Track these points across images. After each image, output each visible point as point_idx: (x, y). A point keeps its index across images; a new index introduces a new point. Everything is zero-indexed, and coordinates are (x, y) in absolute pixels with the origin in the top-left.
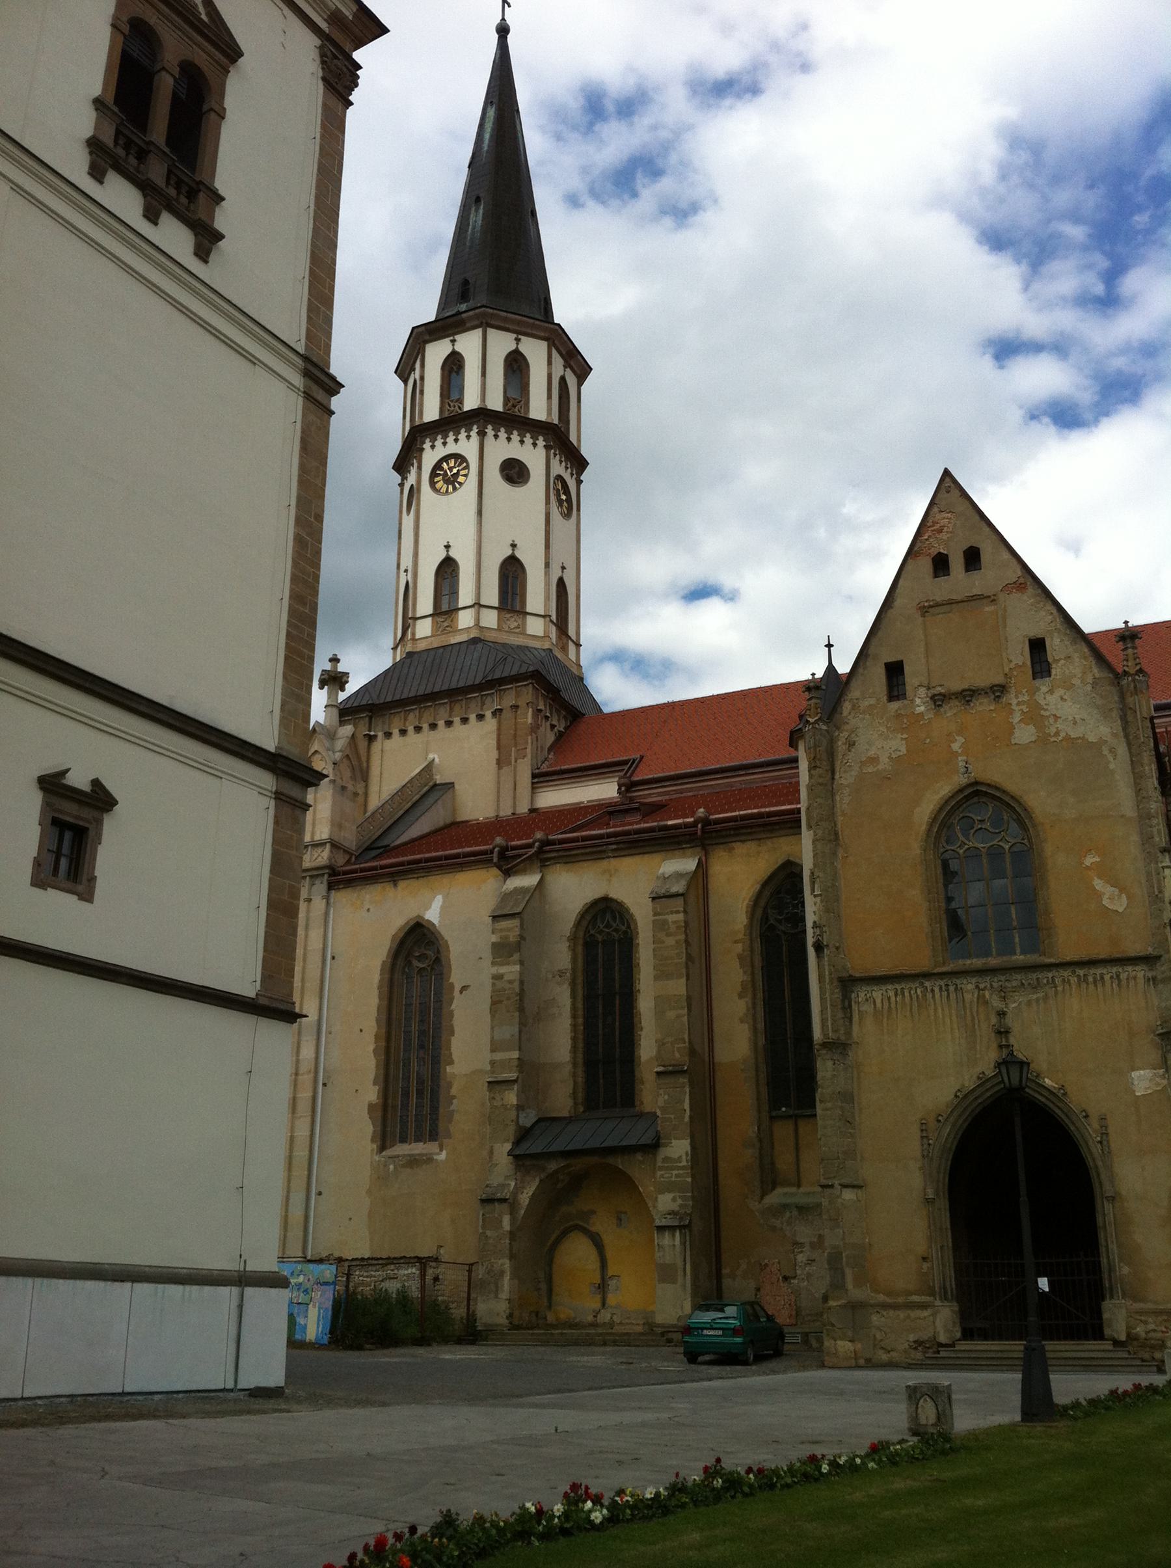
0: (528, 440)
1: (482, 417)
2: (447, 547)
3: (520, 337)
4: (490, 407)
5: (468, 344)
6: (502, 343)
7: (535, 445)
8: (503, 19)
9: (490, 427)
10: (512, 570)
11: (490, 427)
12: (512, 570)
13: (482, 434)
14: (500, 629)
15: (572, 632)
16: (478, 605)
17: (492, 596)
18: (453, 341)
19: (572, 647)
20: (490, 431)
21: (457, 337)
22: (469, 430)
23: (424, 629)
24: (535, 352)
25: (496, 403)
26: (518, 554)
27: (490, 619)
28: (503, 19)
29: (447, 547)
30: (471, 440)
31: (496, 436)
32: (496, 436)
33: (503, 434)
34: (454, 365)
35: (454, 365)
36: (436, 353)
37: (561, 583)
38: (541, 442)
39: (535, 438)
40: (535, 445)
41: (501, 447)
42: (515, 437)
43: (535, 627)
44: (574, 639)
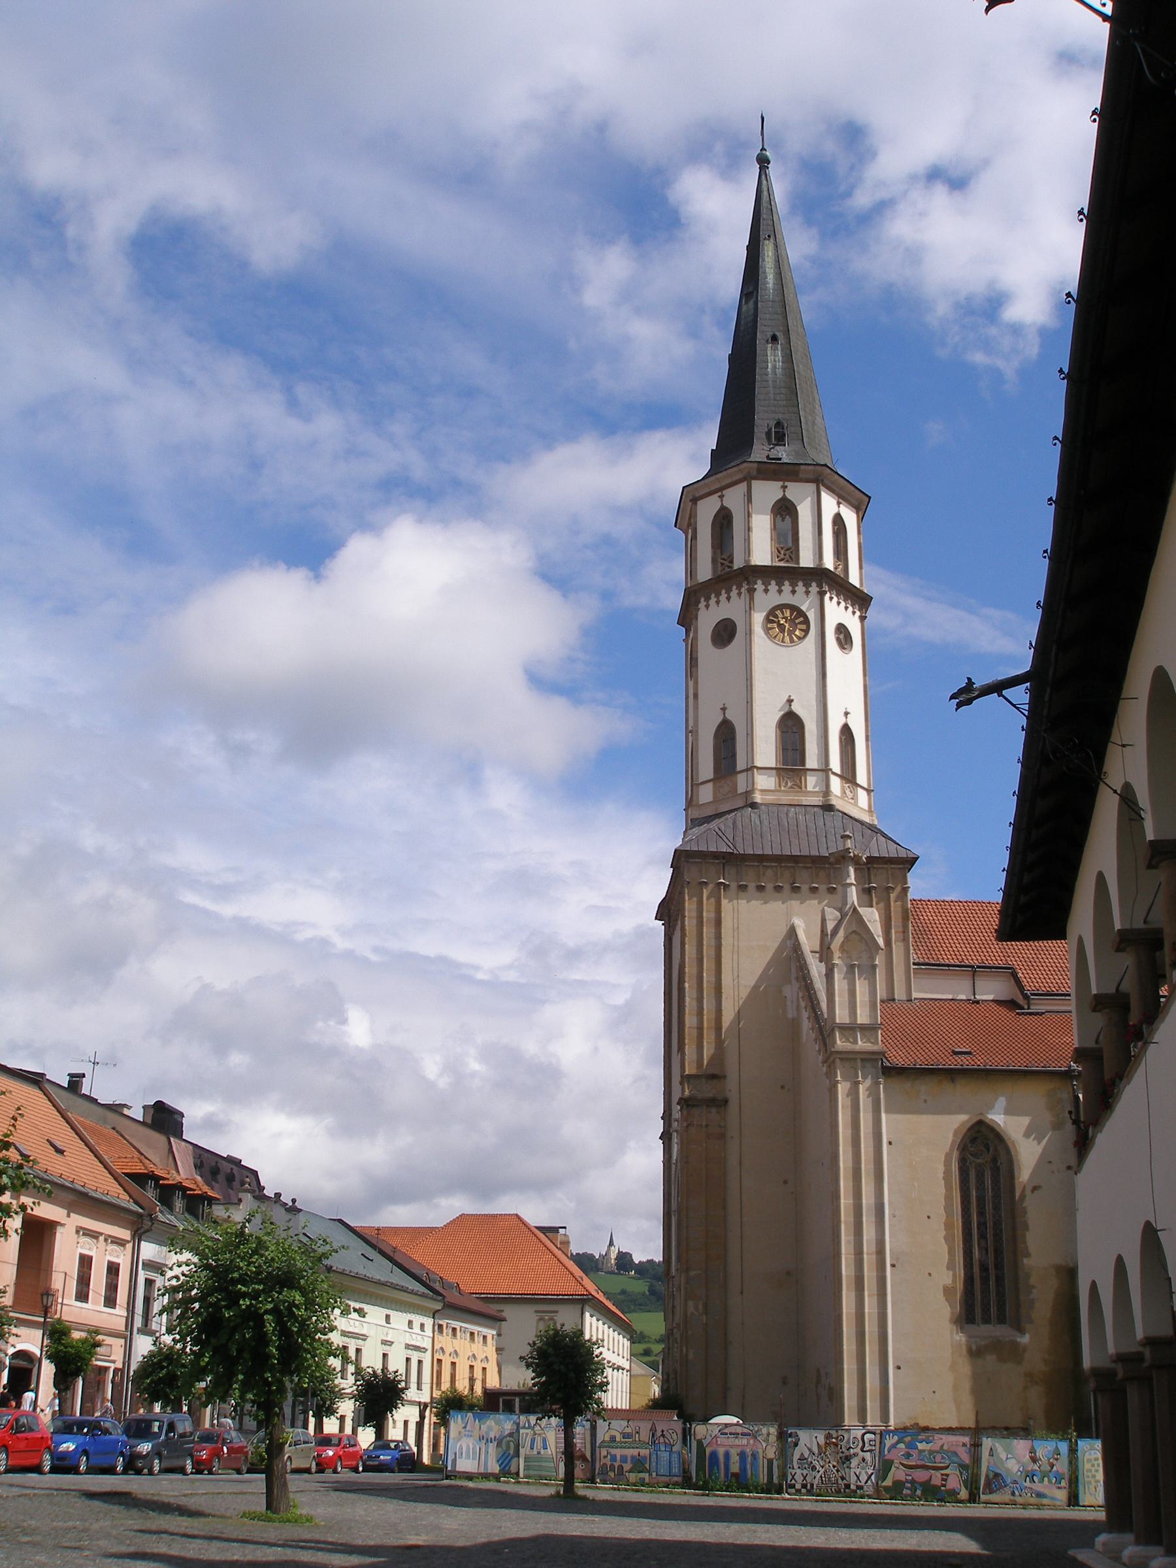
0: (800, 588)
1: (753, 573)
5: (734, 498)
7: (807, 593)
9: (759, 582)
10: (791, 725)
11: (759, 582)
12: (791, 725)
18: (721, 497)
20: (759, 586)
21: (724, 492)
22: (739, 587)
26: (795, 707)
30: (743, 595)
31: (766, 591)
32: (766, 591)
33: (773, 587)
34: (723, 521)
36: (707, 511)
40: (807, 593)
42: (787, 587)
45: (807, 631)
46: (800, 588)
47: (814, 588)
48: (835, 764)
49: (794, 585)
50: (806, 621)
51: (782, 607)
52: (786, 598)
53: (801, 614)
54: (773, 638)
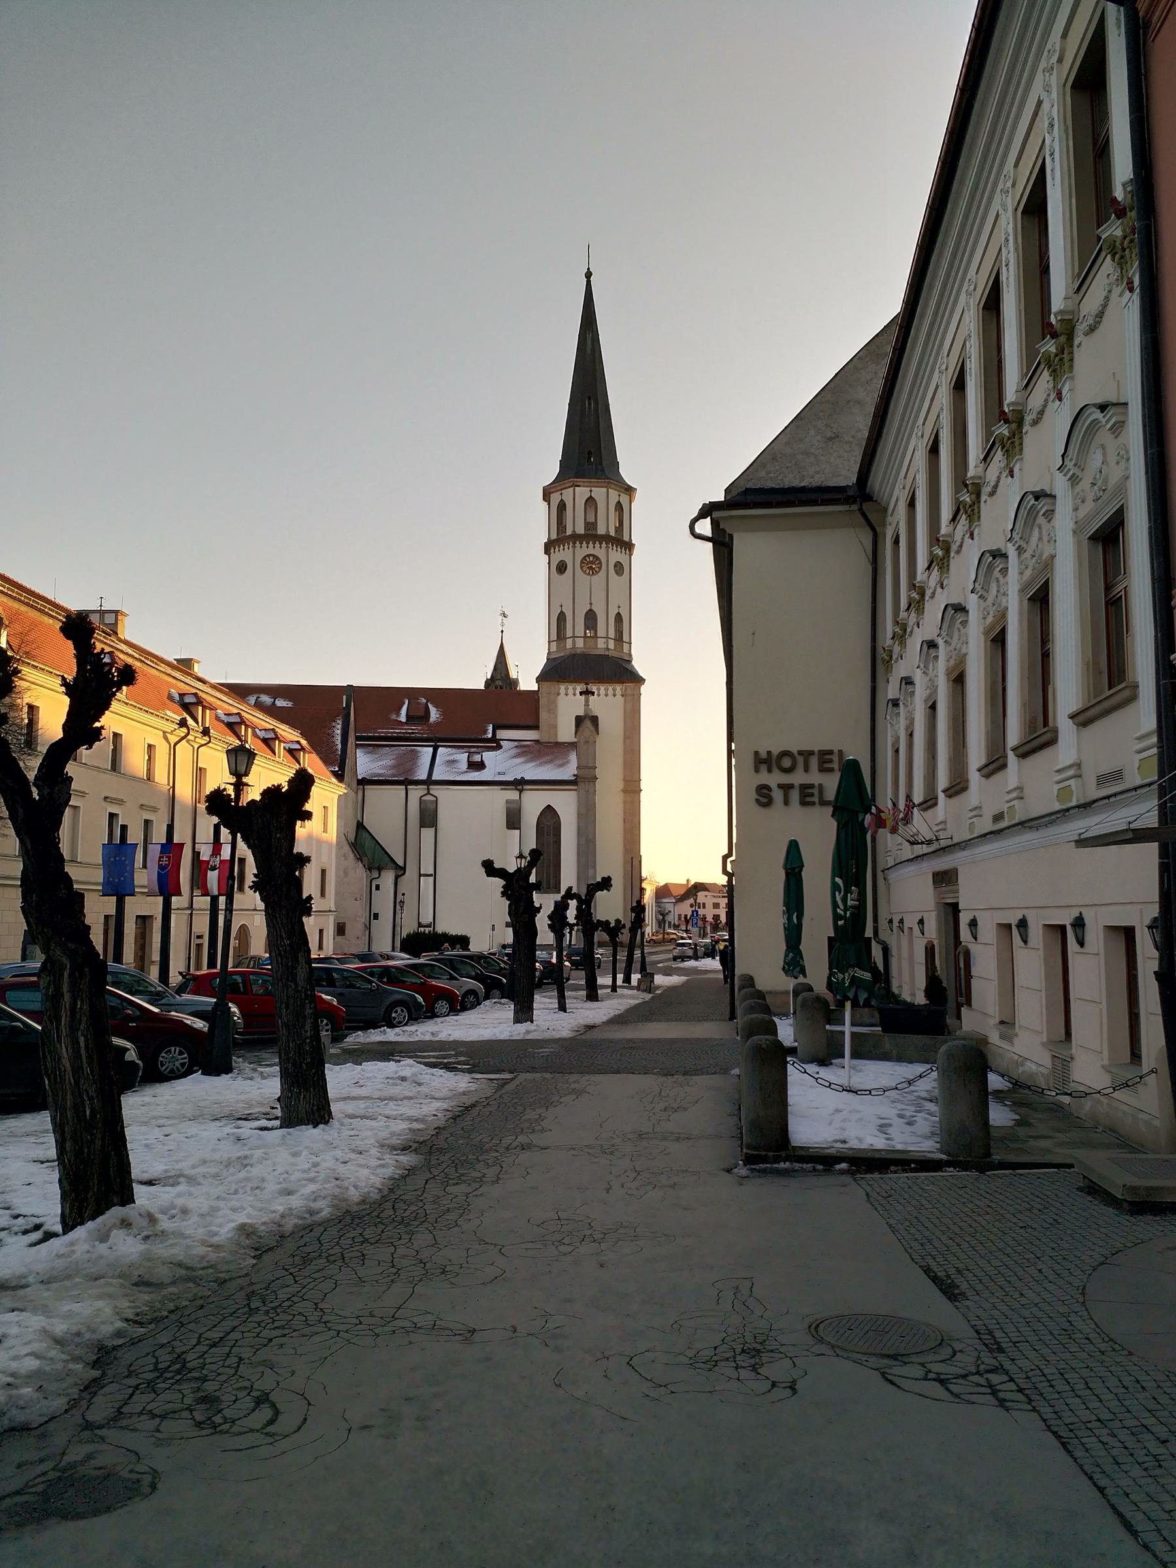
0: (597, 545)
1: (575, 538)
2: (561, 606)
3: (593, 489)
4: (577, 532)
5: (567, 495)
6: (582, 493)
8: (588, 269)
10: (591, 618)
12: (591, 618)
13: (574, 547)
14: (584, 647)
15: (625, 638)
16: (574, 637)
17: (580, 630)
18: (561, 494)
19: (626, 646)
23: (554, 648)
24: (599, 493)
25: (581, 530)
26: (593, 608)
27: (580, 643)
28: (588, 269)
29: (561, 606)
34: (562, 506)
35: (562, 506)
37: (619, 618)
38: (604, 545)
39: (601, 543)
40: (601, 547)
41: (583, 550)
43: (601, 644)
44: (628, 641)
45: (600, 568)
46: (597, 545)
47: (604, 545)
48: (612, 634)
49: (594, 544)
50: (600, 563)
51: (589, 556)
52: (591, 551)
53: (598, 558)
54: (585, 572)
